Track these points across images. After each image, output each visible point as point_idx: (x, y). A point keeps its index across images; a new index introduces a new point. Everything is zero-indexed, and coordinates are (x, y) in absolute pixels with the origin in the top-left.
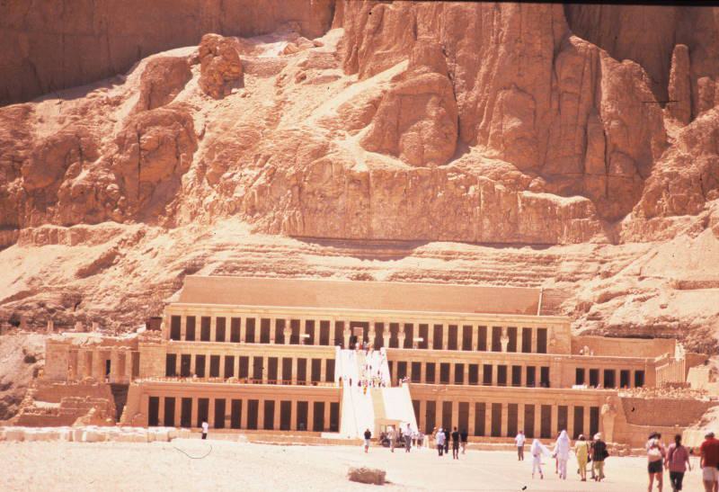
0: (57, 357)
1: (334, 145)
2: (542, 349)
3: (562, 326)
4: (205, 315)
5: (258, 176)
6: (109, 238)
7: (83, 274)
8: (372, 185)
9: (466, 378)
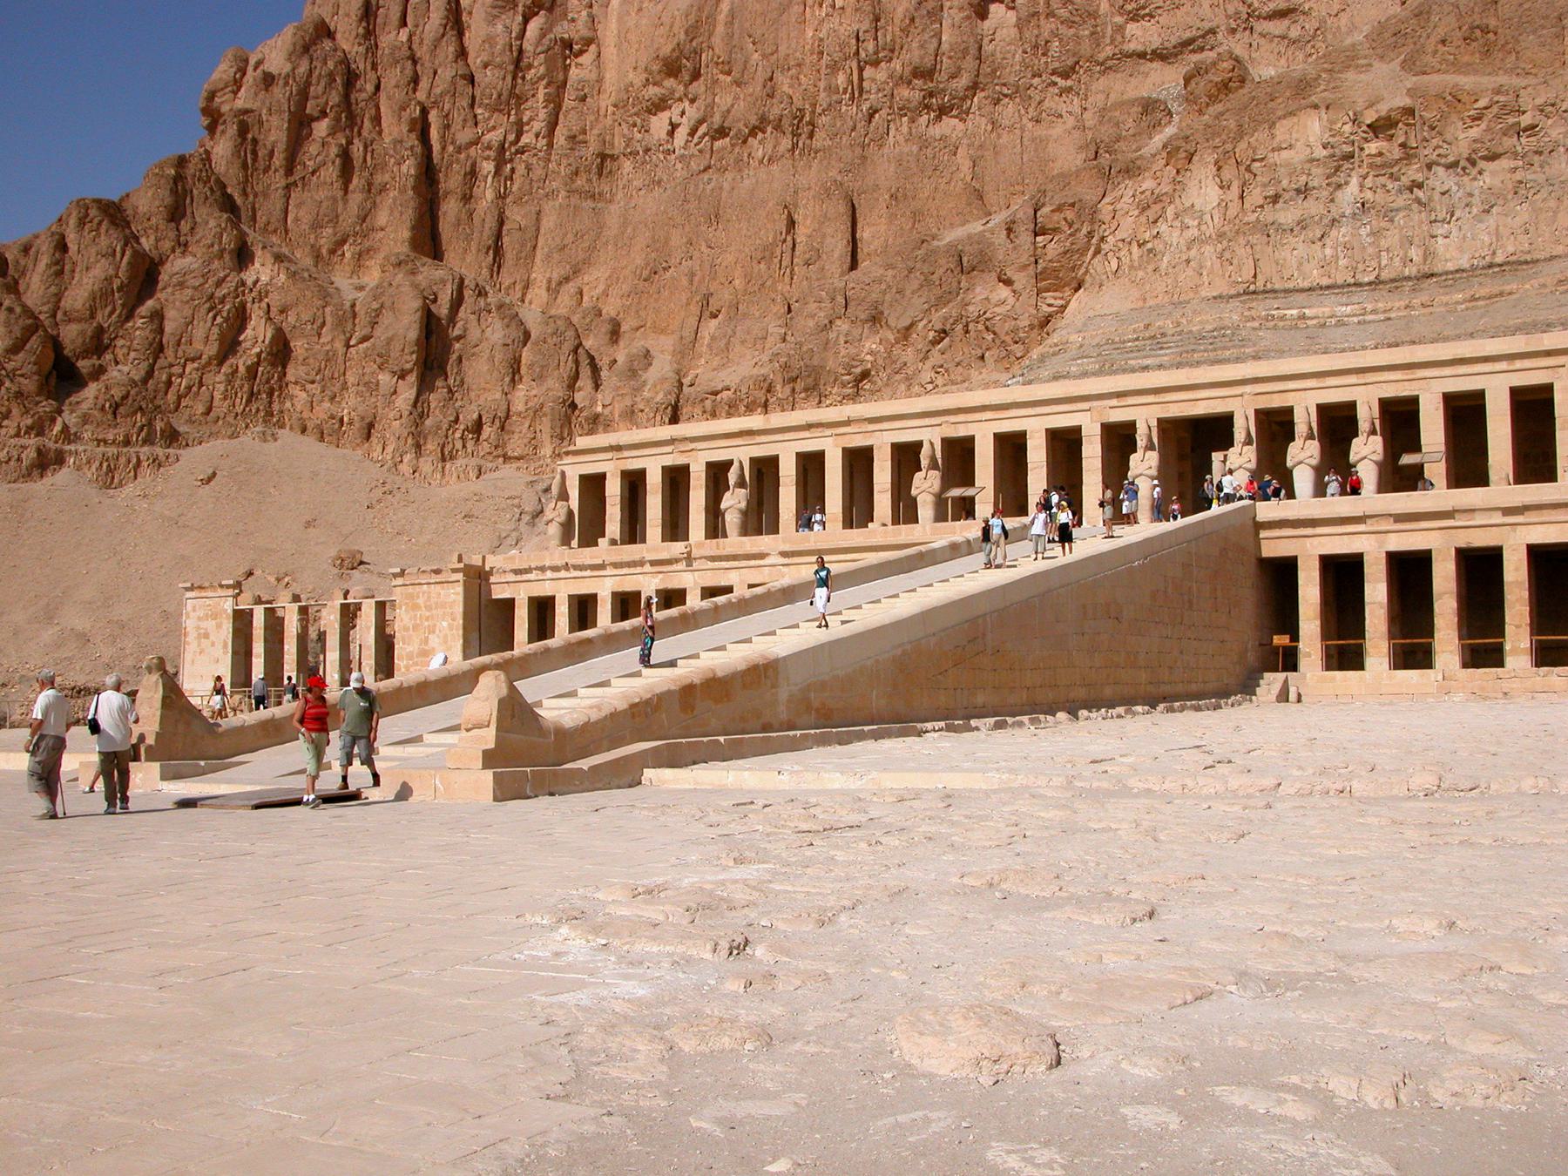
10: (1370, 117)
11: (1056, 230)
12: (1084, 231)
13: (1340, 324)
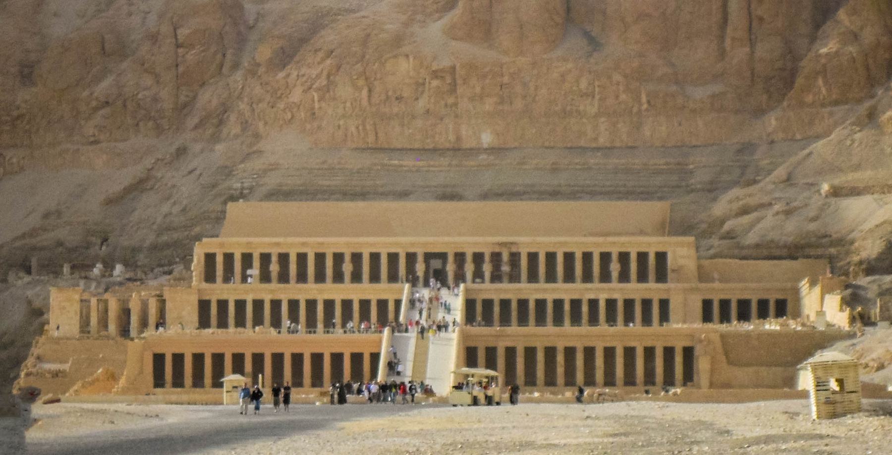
0: (64, 308)
2: (661, 276)
6: (141, 158)
7: (110, 202)
8: (459, 81)
9: (231, 319)
11: (192, 46)
13: (417, 171)
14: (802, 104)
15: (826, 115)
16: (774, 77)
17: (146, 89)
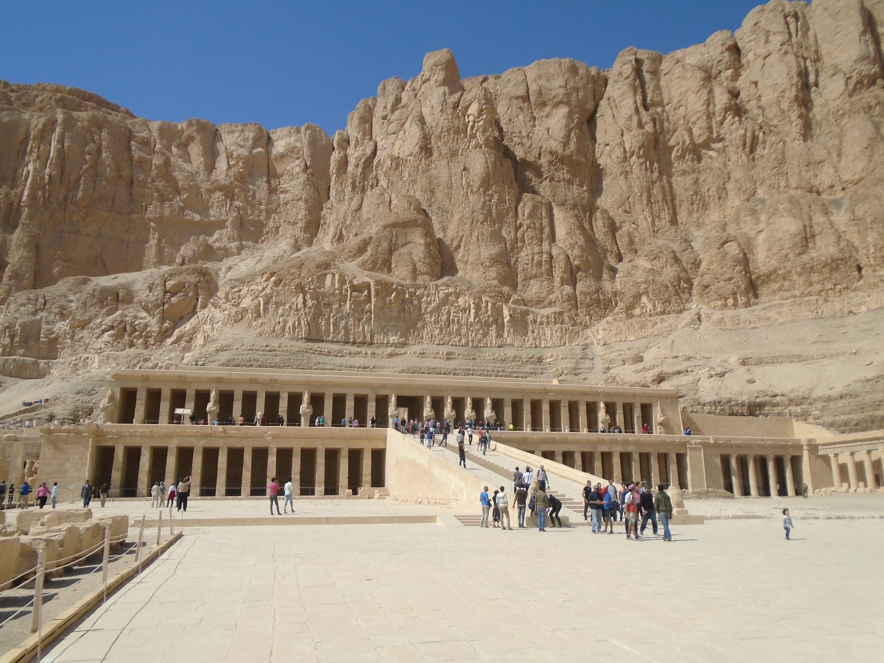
1: (335, 265)
3: (669, 401)
4: (175, 386)
5: (264, 289)
8: (373, 293)
10: (355, 282)
12: (190, 294)
14: (630, 316)
15: (658, 321)
16: (591, 305)
17: (141, 318)
